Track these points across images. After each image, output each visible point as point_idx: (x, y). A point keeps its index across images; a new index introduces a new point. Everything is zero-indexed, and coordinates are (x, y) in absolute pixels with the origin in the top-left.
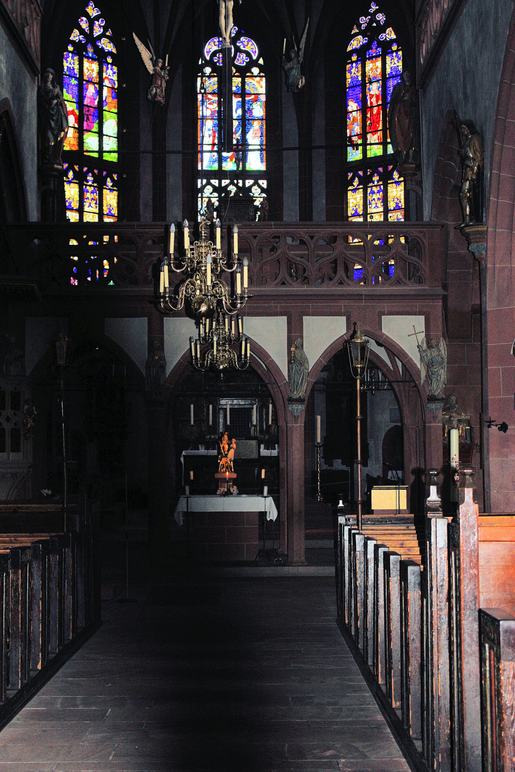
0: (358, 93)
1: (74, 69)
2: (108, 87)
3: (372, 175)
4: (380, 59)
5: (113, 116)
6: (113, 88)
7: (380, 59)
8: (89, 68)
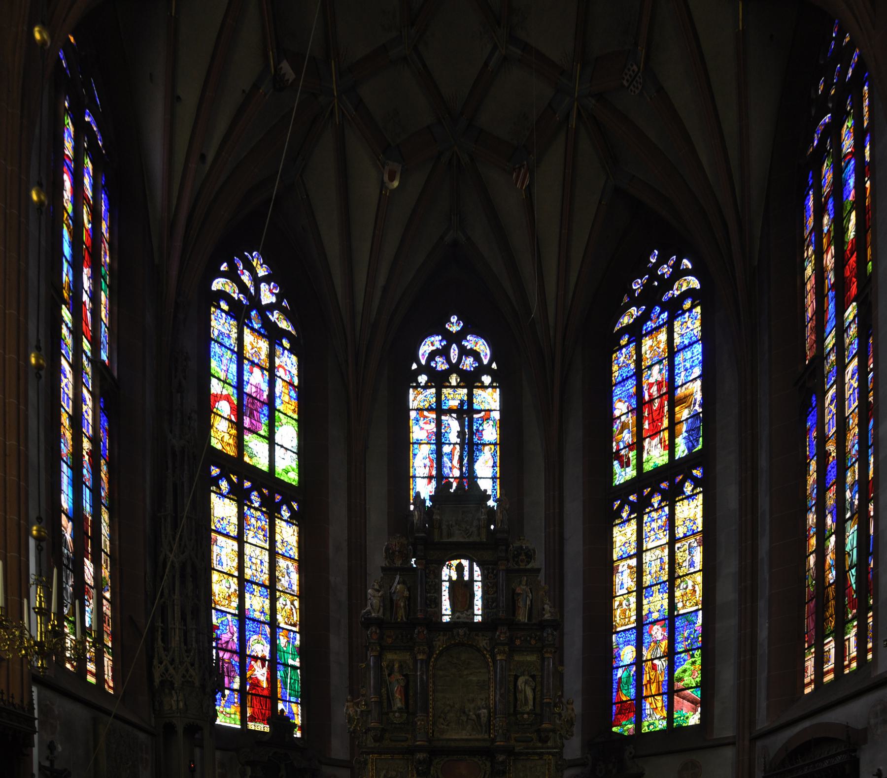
0: (629, 387)
1: (229, 337)
2: (283, 380)
3: (651, 495)
4: (664, 329)
7: (664, 329)
8: (255, 344)
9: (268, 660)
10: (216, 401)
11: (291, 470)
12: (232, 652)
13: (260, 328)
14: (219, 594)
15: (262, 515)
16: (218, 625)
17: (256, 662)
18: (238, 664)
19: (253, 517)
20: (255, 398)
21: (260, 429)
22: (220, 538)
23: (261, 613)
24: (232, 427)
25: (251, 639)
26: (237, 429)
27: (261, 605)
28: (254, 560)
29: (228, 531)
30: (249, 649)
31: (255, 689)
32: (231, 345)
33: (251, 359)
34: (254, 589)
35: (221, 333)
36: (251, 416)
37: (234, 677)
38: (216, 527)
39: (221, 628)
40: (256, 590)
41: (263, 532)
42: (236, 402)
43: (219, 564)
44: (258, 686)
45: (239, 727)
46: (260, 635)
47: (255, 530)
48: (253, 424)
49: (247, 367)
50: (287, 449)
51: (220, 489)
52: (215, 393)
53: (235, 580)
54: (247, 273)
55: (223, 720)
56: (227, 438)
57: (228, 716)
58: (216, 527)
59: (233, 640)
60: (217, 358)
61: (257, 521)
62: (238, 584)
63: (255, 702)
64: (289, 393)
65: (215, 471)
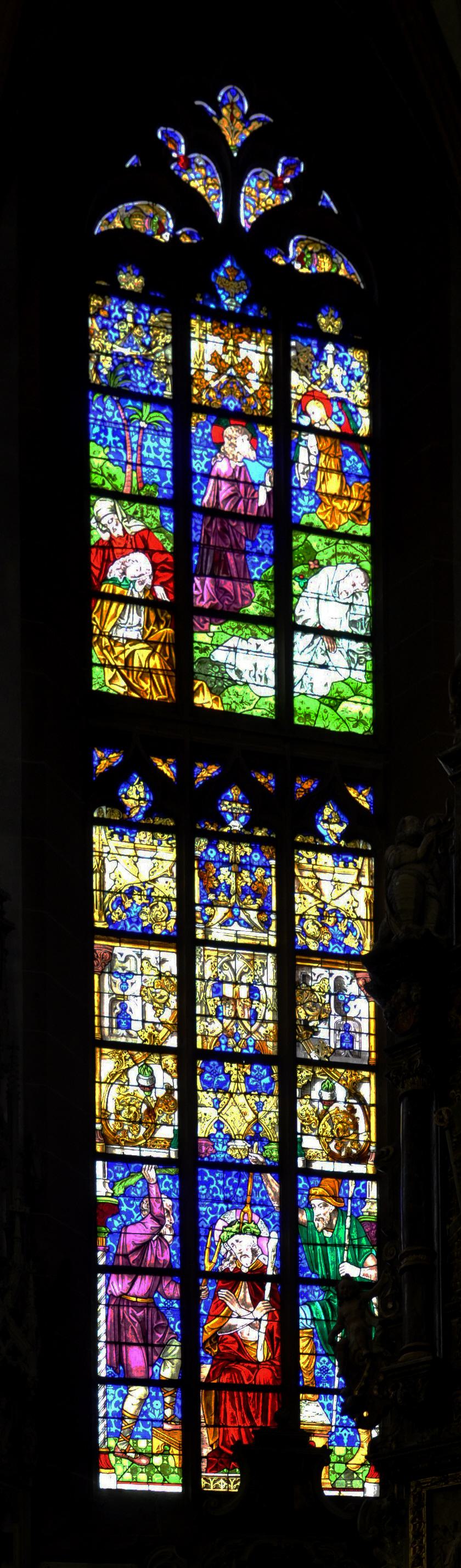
1: (146, 363)
2: (320, 433)
5: (350, 550)
6: (347, 437)
8: (227, 359)
9: (270, 1278)
10: (108, 562)
11: (347, 692)
12: (159, 1272)
13: (244, 304)
14: (118, 1113)
15: (254, 850)
16: (114, 1200)
17: (233, 1290)
18: (176, 1306)
19: (227, 864)
20: (233, 515)
21: (248, 599)
22: (123, 950)
23: (251, 1140)
24: (158, 622)
25: (220, 1225)
26: (174, 624)
27: (250, 1117)
28: (228, 990)
29: (145, 924)
30: (211, 1253)
31: (230, 1369)
32: (153, 384)
33: (217, 404)
34: (228, 1076)
35: (121, 362)
36: (219, 570)
37: (164, 1346)
38: (108, 920)
39: (124, 1208)
40: (234, 1077)
41: (259, 901)
42: (169, 546)
43: (118, 1027)
44: (239, 1360)
45: (179, 1489)
46: (247, 1209)
47: (233, 900)
48: (226, 592)
49: (200, 427)
50: (334, 635)
51: (123, 808)
52: (106, 537)
53: (169, 1060)
54: (200, 159)
55: (128, 1477)
56: (141, 655)
57: (144, 1461)
58: (108, 920)
59: (161, 1236)
60: (110, 438)
61: (238, 874)
62: (179, 1070)
63: (230, 1410)
64: (342, 464)
65: (105, 760)
